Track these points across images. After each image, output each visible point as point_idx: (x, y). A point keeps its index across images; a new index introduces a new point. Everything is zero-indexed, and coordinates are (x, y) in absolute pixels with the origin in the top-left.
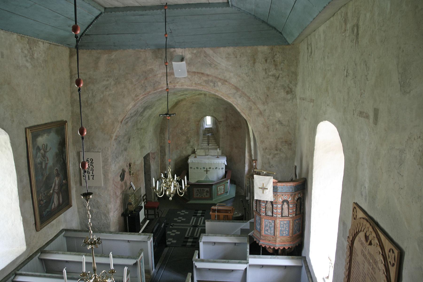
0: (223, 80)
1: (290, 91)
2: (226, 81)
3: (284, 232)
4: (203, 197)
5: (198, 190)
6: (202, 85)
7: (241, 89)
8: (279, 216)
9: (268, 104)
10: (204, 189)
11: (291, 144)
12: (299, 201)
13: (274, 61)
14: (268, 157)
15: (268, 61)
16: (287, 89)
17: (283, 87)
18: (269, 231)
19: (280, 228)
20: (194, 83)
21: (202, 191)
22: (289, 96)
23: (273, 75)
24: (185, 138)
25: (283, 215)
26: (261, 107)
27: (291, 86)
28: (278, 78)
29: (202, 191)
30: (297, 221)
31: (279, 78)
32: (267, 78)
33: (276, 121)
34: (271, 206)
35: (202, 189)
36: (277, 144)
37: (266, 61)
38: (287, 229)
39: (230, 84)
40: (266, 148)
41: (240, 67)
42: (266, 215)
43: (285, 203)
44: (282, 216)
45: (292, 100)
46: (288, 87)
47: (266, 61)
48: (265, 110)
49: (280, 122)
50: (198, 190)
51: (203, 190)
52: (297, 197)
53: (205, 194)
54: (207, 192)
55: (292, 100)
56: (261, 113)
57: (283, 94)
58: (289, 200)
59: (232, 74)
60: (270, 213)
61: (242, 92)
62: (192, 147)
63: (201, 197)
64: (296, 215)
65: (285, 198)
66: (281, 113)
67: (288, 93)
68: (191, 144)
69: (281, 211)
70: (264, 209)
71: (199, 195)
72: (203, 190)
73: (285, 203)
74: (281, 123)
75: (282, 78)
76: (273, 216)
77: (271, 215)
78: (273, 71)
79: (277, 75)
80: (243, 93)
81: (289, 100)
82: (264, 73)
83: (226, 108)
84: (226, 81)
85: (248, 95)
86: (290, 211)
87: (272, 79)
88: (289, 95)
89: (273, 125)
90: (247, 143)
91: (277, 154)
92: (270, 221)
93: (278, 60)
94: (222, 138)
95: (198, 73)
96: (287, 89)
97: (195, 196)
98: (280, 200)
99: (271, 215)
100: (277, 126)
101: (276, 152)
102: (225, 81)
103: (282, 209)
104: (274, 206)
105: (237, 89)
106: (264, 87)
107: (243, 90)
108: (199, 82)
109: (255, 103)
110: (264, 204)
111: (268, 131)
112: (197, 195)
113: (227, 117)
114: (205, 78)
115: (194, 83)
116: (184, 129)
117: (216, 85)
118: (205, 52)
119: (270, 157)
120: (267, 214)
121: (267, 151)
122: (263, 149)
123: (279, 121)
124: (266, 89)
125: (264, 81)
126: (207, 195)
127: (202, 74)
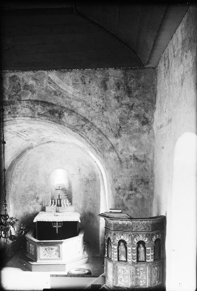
0: (69, 110)
1: (146, 122)
2: (74, 112)
4: (52, 257)
6: (45, 116)
7: (90, 120)
8: (134, 261)
9: (120, 136)
11: (148, 183)
12: (157, 243)
13: (128, 87)
14: (122, 198)
15: (121, 87)
16: (143, 119)
17: (137, 116)
18: (123, 280)
19: (136, 277)
20: (36, 113)
22: (145, 128)
23: (127, 104)
25: (139, 260)
26: (113, 140)
27: (147, 115)
28: (132, 107)
30: (156, 268)
31: (133, 107)
32: (120, 107)
33: (130, 156)
34: (125, 249)
36: (131, 183)
37: (119, 87)
38: (145, 278)
39: (77, 114)
40: (119, 188)
41: (89, 95)
42: (118, 260)
43: (141, 245)
45: (149, 132)
46: (144, 117)
47: (119, 87)
48: (118, 144)
49: (135, 158)
52: (154, 238)
55: (149, 132)
56: (113, 148)
57: (137, 124)
58: (145, 241)
59: (80, 104)
60: (123, 258)
61: (91, 123)
64: (154, 260)
65: (141, 238)
66: (136, 147)
67: (143, 123)
69: (136, 254)
73: (141, 245)
74: (137, 159)
75: (137, 106)
76: (126, 261)
77: (125, 260)
78: (127, 100)
79: (131, 104)
80: (92, 124)
81: (145, 132)
82: (116, 102)
84: (74, 112)
85: (99, 126)
86: (147, 254)
87: (124, 108)
88: (145, 126)
89: (127, 161)
91: (133, 194)
92: (124, 268)
93: (132, 86)
95: (41, 101)
96: (143, 119)
97: (41, 257)
100: (132, 162)
101: (131, 192)
102: (72, 111)
103: (138, 252)
105: (85, 120)
106: (117, 117)
107: (93, 122)
108: (42, 113)
109: (106, 136)
111: (122, 167)
114: (49, 108)
115: (36, 113)
117: (62, 116)
118: (49, 78)
119: (124, 198)
120: (120, 259)
121: (120, 190)
122: (116, 189)
123: (134, 156)
124: (118, 119)
125: (117, 111)
127: (46, 102)
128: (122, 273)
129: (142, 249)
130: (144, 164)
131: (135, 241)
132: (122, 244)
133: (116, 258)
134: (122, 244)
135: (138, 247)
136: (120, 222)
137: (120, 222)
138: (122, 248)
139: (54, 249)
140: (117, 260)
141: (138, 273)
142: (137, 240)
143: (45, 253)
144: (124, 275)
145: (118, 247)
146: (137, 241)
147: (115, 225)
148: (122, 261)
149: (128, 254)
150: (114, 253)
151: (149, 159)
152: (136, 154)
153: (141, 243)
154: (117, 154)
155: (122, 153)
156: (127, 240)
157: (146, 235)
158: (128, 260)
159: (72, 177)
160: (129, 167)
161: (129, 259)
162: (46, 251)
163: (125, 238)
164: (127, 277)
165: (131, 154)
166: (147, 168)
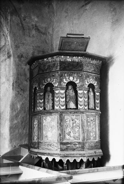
3: (92, 134)
18: (72, 134)
33: (32, 25)
34: (74, 94)
38: (94, 130)
40: (22, 56)
44: (89, 109)
60: (72, 105)
69: (87, 99)
70: (64, 99)
74: (38, 30)
76: (77, 108)
77: (75, 107)
98: (86, 82)
99: (75, 107)
104: (79, 92)
110: (63, 92)
120: (68, 107)
122: (18, 57)
123: (36, 26)
128: (71, 125)
129: (92, 94)
130: (45, 36)
131: (86, 82)
132: (70, 87)
133: (63, 106)
134: (70, 87)
135: (89, 91)
136: (69, 59)
137: (69, 59)
138: (71, 93)
140: (64, 107)
141: (89, 124)
142: (88, 82)
144: (73, 127)
145: (66, 92)
146: (88, 84)
147: (61, 63)
148: (71, 109)
149: (79, 98)
150: (61, 99)
151: (49, 33)
152: (38, 25)
153: (91, 86)
154: (20, 19)
155: (25, 20)
156: (77, 82)
157: (96, 78)
158: (79, 106)
160: (31, 35)
161: (81, 106)
163: (75, 79)
164: (77, 130)
165: (34, 23)
166: (47, 41)
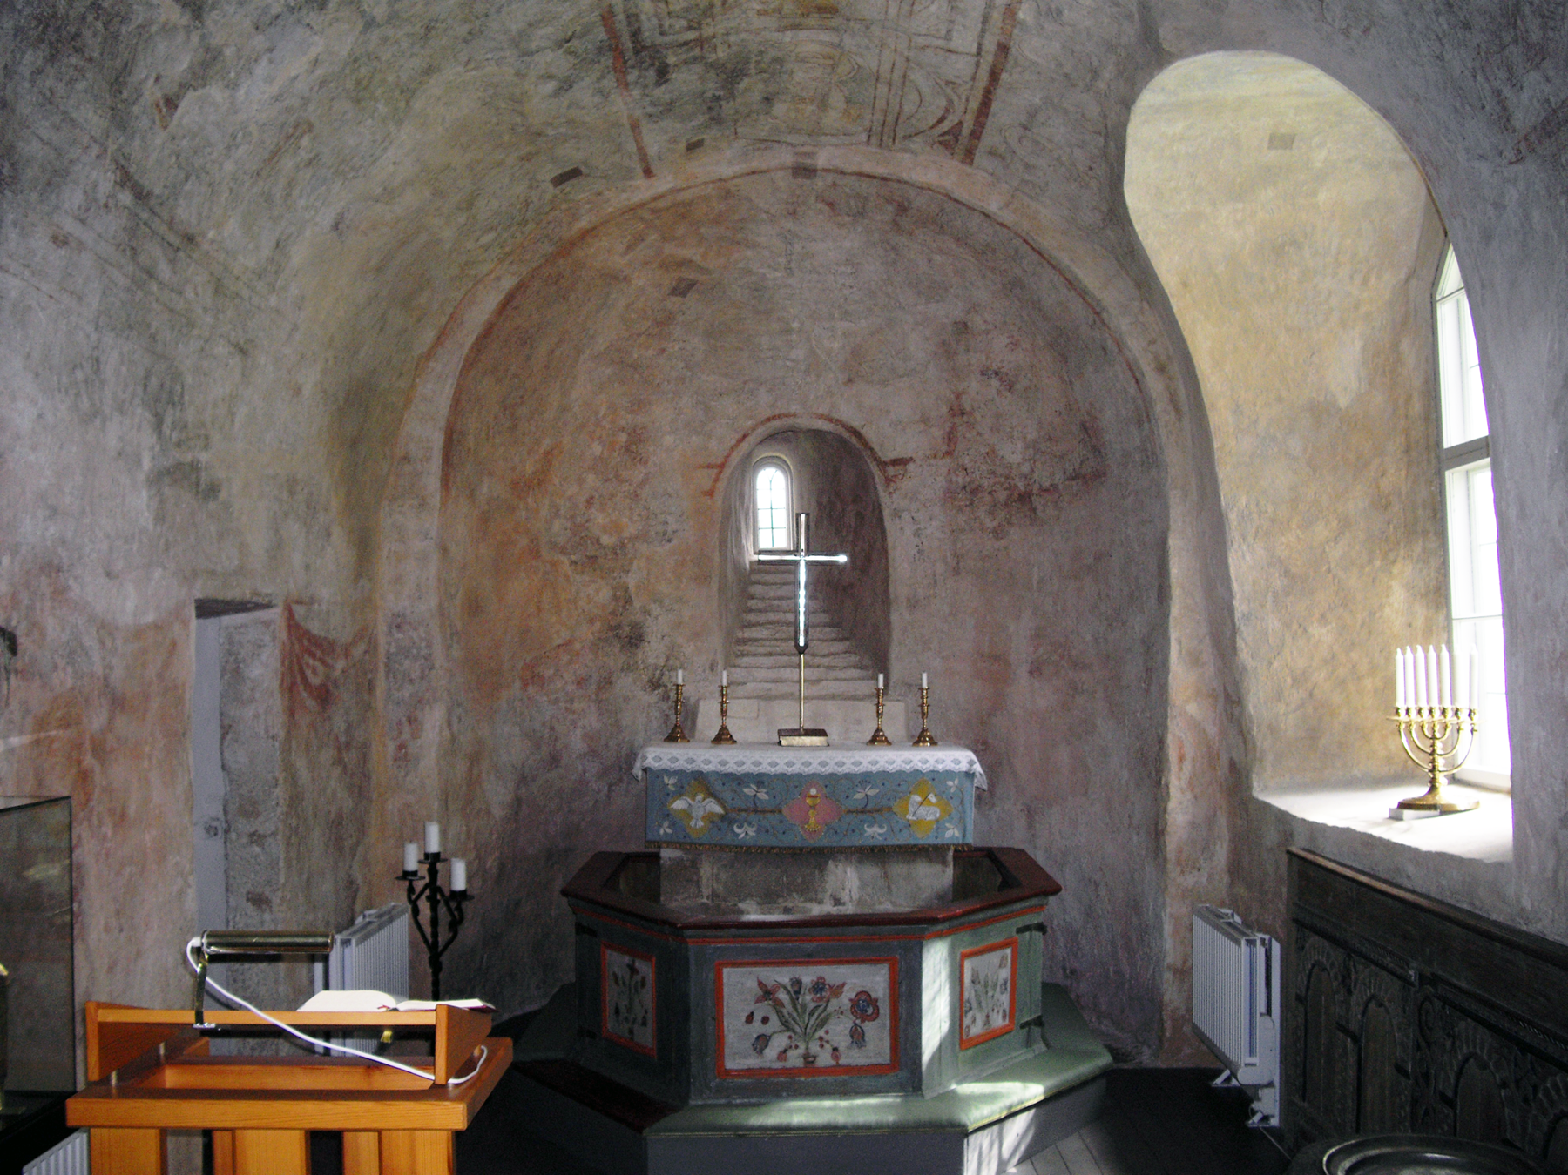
5: (767, 993)
10: (833, 974)
21: (807, 998)
24: (600, 594)
29: (807, 998)
35: (808, 975)
50: (767, 993)
51: (819, 986)
53: (839, 1031)
54: (864, 1006)
62: (655, 684)
63: (795, 1060)
68: (653, 652)
71: (779, 1042)
72: (819, 986)
83: (963, 328)
90: (1180, 568)
94: (913, 604)
112: (762, 1042)
113: (957, 411)
116: (600, 518)
126: (858, 1037)
139: (837, 990)
143: (757, 1028)
159: (888, 481)
162: (764, 1009)
